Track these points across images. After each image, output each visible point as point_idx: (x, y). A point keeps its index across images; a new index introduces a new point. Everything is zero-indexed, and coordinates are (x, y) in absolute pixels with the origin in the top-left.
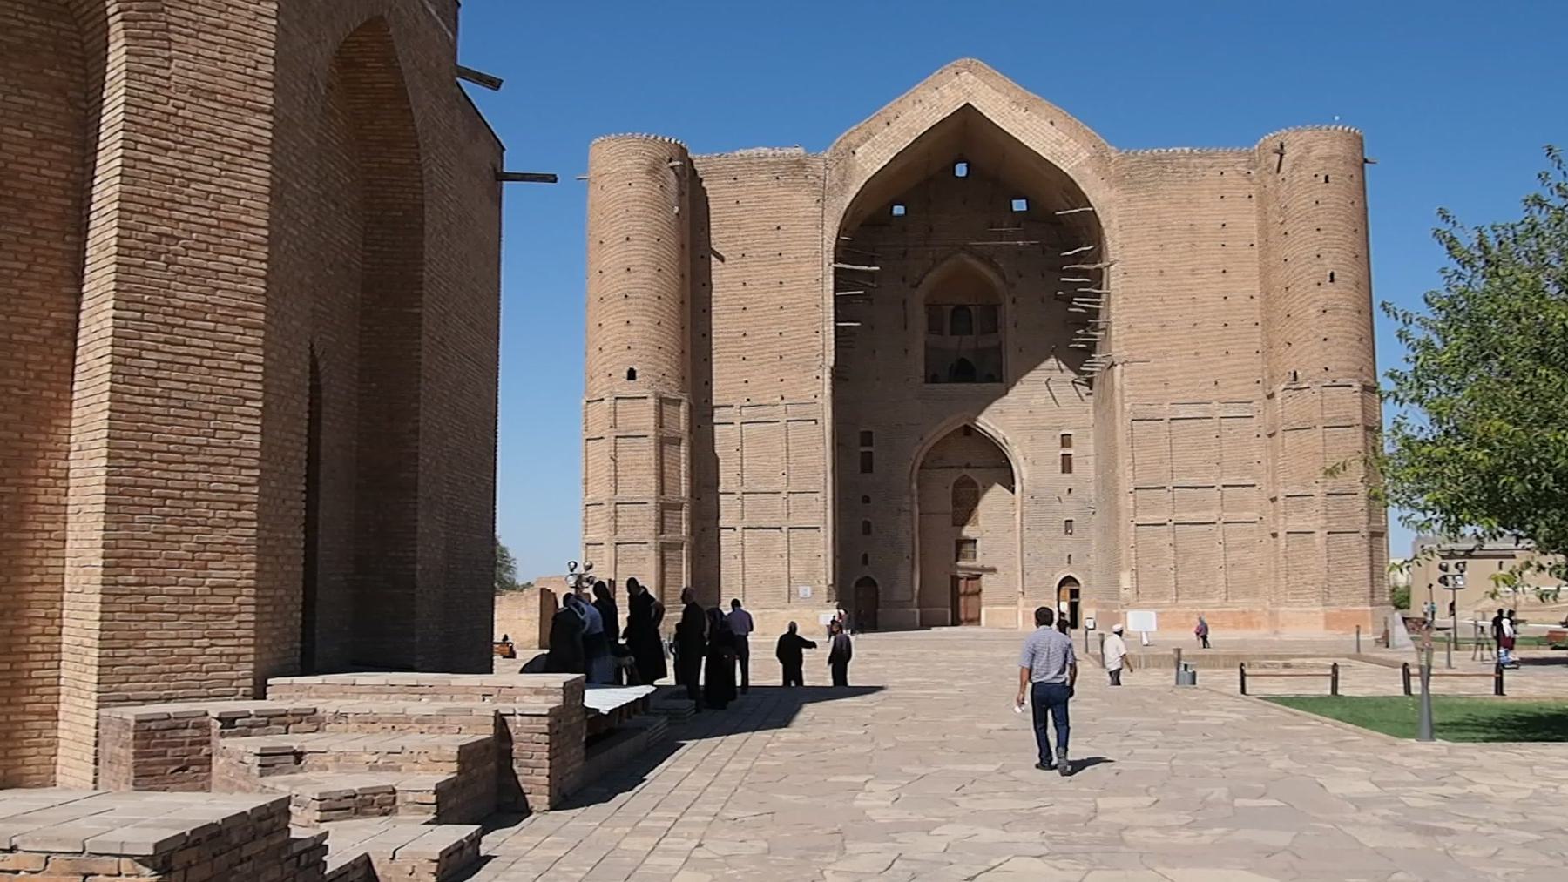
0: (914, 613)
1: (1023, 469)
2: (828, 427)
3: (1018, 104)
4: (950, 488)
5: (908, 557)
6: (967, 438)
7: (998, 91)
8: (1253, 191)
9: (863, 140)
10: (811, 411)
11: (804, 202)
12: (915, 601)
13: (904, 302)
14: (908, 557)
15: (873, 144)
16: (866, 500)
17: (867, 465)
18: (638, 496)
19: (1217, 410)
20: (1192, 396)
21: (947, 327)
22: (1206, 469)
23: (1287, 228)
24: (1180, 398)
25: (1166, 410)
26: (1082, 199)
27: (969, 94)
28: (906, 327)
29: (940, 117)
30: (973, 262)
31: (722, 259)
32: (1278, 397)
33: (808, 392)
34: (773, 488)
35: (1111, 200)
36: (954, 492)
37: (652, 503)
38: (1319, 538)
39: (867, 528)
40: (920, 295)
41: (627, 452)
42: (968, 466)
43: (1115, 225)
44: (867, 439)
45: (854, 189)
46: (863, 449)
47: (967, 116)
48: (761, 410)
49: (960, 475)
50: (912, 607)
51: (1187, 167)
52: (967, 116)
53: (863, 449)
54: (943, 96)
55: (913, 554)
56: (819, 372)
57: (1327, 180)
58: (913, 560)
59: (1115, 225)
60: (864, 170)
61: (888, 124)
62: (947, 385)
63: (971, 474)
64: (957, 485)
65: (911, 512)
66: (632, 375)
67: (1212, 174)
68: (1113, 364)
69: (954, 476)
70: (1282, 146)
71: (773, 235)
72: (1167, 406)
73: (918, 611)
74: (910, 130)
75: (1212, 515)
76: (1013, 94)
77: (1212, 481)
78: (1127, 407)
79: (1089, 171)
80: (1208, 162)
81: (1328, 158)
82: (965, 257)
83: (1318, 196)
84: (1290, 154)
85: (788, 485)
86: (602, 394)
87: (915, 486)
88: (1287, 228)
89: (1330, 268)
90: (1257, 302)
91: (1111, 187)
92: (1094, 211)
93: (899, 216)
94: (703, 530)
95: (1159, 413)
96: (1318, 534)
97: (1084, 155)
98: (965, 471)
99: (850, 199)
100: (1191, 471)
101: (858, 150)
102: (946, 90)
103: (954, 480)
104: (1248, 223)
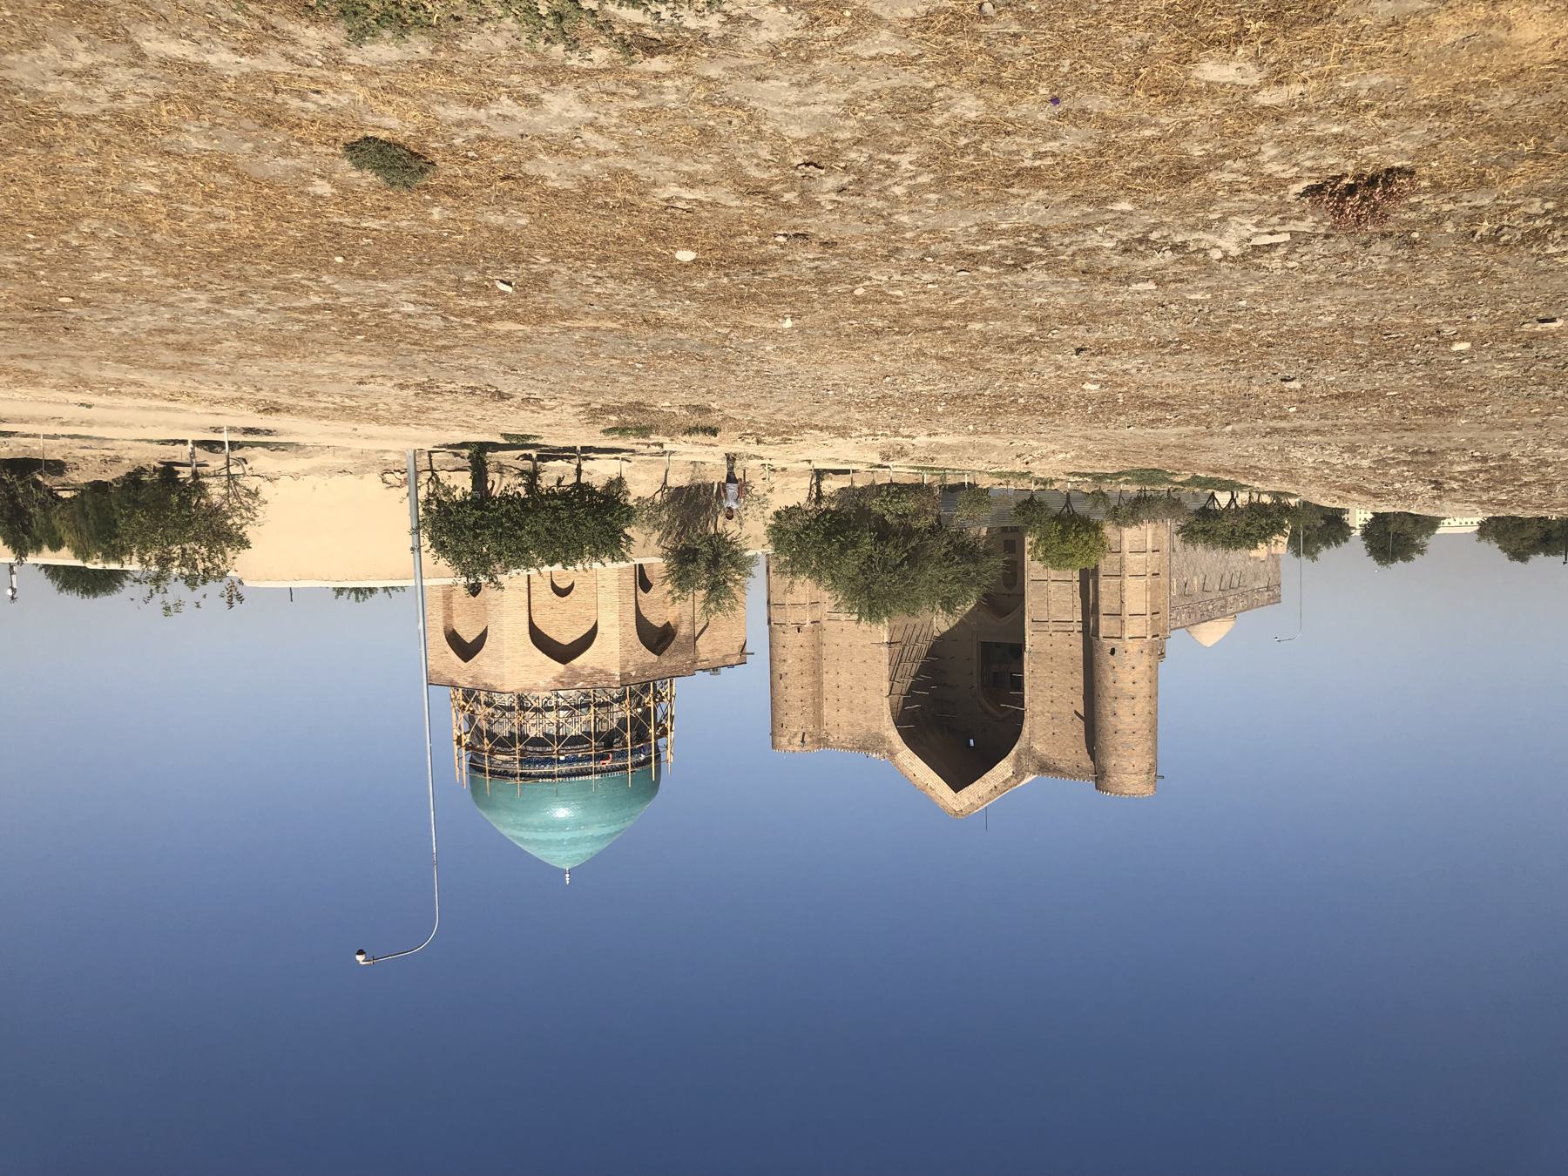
2: (1026, 617)
8: (825, 727)
11: (1038, 747)
18: (1108, 580)
26: (900, 732)
29: (970, 787)
31: (1076, 713)
32: (808, 622)
33: (1038, 638)
34: (1056, 583)
35: (887, 730)
37: (1101, 576)
42: (1009, 595)
45: (1013, 752)
47: (957, 787)
48: (1065, 629)
52: (957, 787)
54: (969, 798)
66: (1113, 652)
67: (842, 738)
68: (890, 643)
83: (786, 718)
84: (798, 740)
86: (1131, 641)
90: (825, 670)
92: (896, 725)
97: (899, 755)
99: (1017, 745)
102: (967, 803)
104: (828, 711)
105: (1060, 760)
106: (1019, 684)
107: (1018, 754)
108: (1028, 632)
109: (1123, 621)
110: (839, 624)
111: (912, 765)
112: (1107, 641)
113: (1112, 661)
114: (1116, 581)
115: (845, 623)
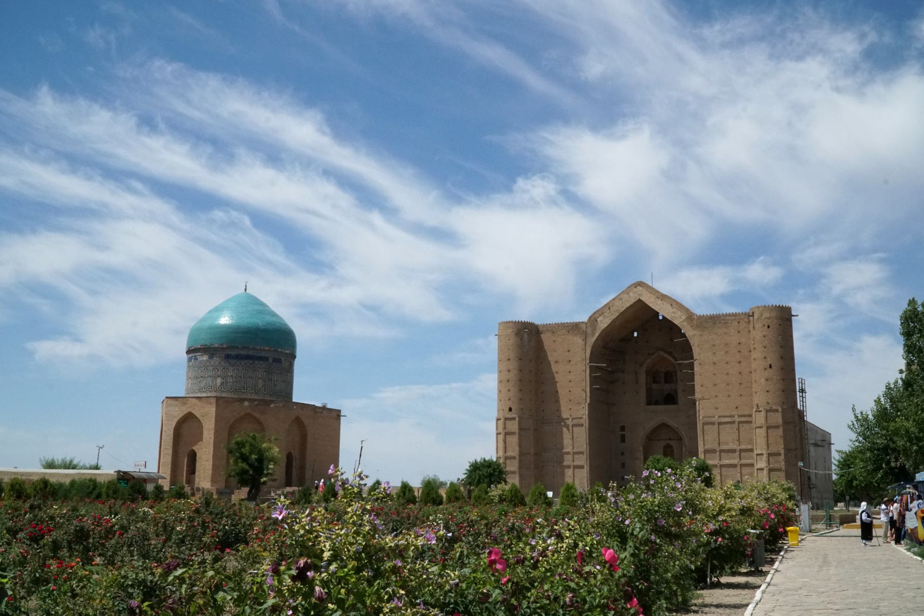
1: (686, 441)
3: (659, 298)
7: (651, 293)
9: (600, 315)
10: (582, 421)
11: (578, 340)
13: (637, 373)
15: (604, 317)
16: (623, 454)
17: (623, 439)
19: (737, 419)
20: (727, 414)
21: (663, 380)
22: (733, 442)
23: (755, 346)
24: (720, 414)
25: (716, 419)
27: (640, 295)
28: (637, 382)
29: (628, 305)
30: (666, 356)
33: (579, 414)
35: (694, 335)
38: (765, 472)
39: (623, 465)
40: (644, 369)
41: (509, 438)
42: (670, 439)
43: (696, 345)
44: (623, 428)
45: (597, 335)
46: (621, 433)
51: (723, 320)
53: (621, 433)
56: (584, 405)
57: (769, 327)
59: (696, 345)
60: (600, 327)
61: (609, 308)
62: (662, 406)
63: (671, 443)
66: (510, 410)
69: (663, 443)
70: (753, 313)
71: (567, 353)
72: (717, 417)
74: (617, 311)
75: (735, 461)
76: (657, 294)
77: (735, 447)
78: (701, 418)
79: (686, 323)
80: (733, 318)
81: (769, 318)
82: (662, 353)
85: (573, 449)
86: (501, 417)
87: (642, 448)
88: (755, 346)
89: (769, 363)
91: (694, 329)
93: (638, 334)
94: (543, 466)
95: (713, 420)
96: (765, 469)
97: (684, 317)
99: (595, 338)
100: (727, 444)
101: (598, 319)
102: (631, 294)
105: (564, 335)
106: (593, 380)
107: (593, 334)
108: (586, 417)
109: (505, 428)
110: (742, 413)
111: (673, 313)
112: (514, 416)
113: (510, 404)
114: (509, 454)
115: (733, 413)
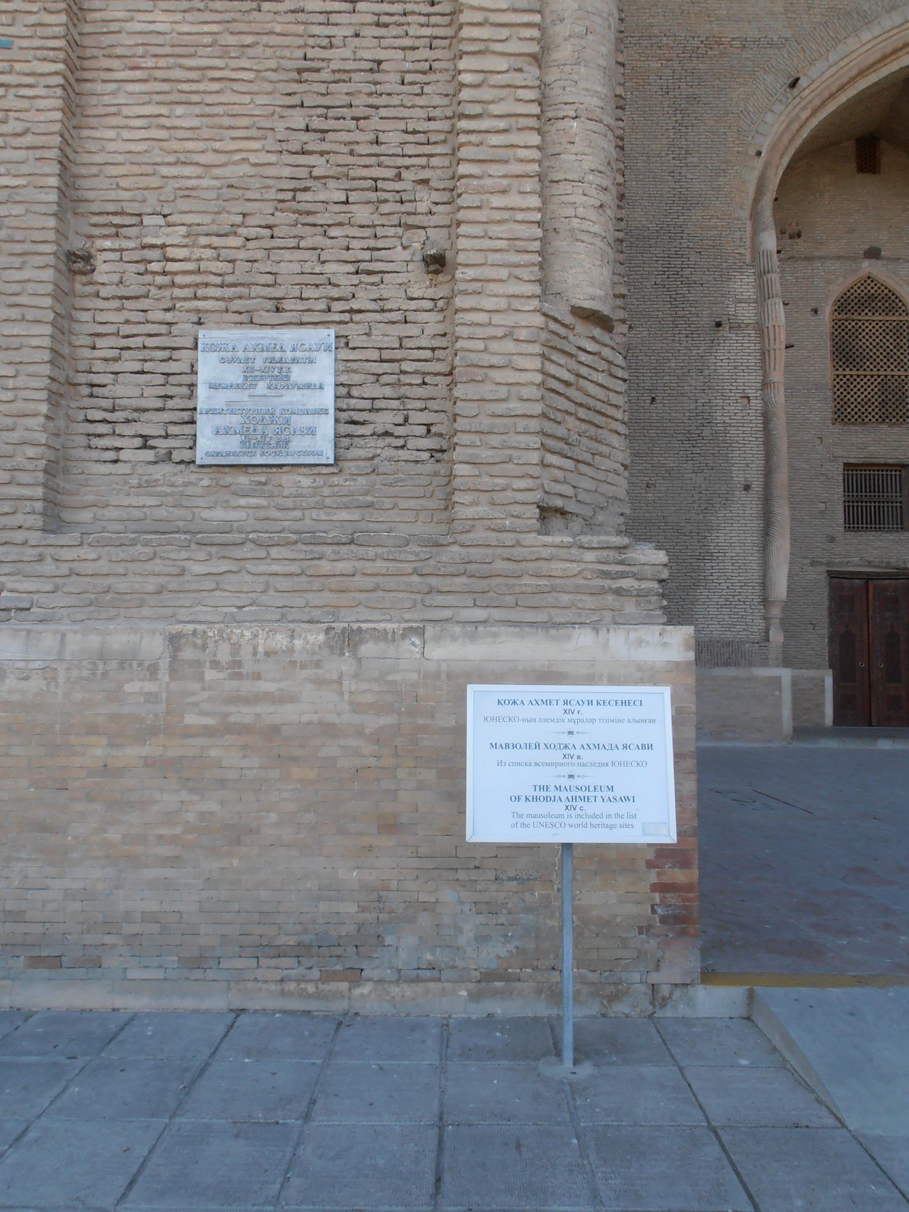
0: (777, 681)
4: (827, 311)
5: (747, 488)
6: (868, 178)
12: (777, 636)
14: (747, 488)
36: (837, 325)
42: (873, 254)
49: (851, 280)
50: (765, 663)
55: (768, 473)
58: (767, 499)
64: (843, 305)
65: (761, 330)
73: (786, 675)
98: (867, 267)
103: (837, 289)
